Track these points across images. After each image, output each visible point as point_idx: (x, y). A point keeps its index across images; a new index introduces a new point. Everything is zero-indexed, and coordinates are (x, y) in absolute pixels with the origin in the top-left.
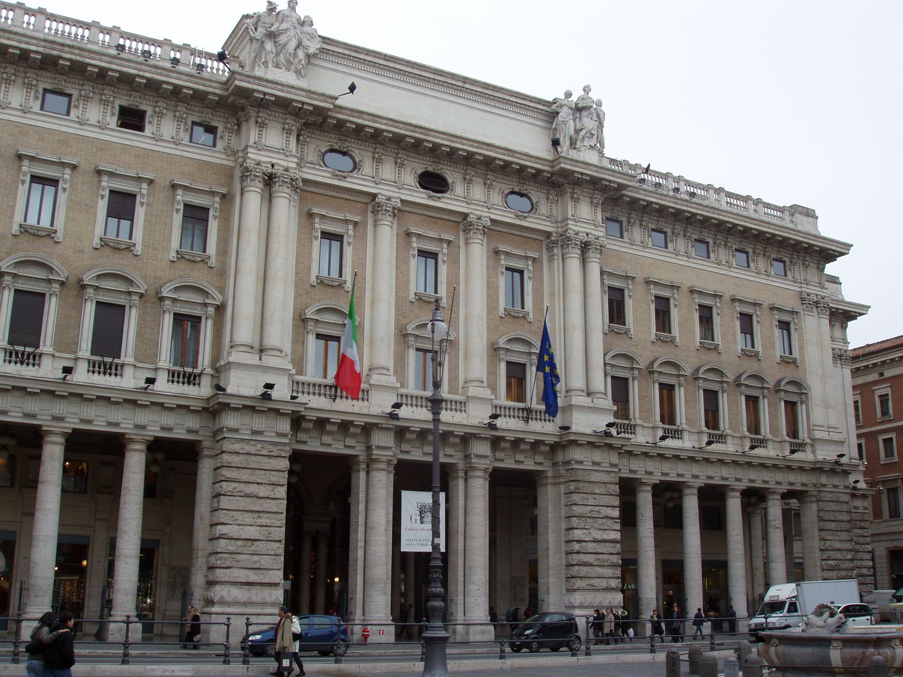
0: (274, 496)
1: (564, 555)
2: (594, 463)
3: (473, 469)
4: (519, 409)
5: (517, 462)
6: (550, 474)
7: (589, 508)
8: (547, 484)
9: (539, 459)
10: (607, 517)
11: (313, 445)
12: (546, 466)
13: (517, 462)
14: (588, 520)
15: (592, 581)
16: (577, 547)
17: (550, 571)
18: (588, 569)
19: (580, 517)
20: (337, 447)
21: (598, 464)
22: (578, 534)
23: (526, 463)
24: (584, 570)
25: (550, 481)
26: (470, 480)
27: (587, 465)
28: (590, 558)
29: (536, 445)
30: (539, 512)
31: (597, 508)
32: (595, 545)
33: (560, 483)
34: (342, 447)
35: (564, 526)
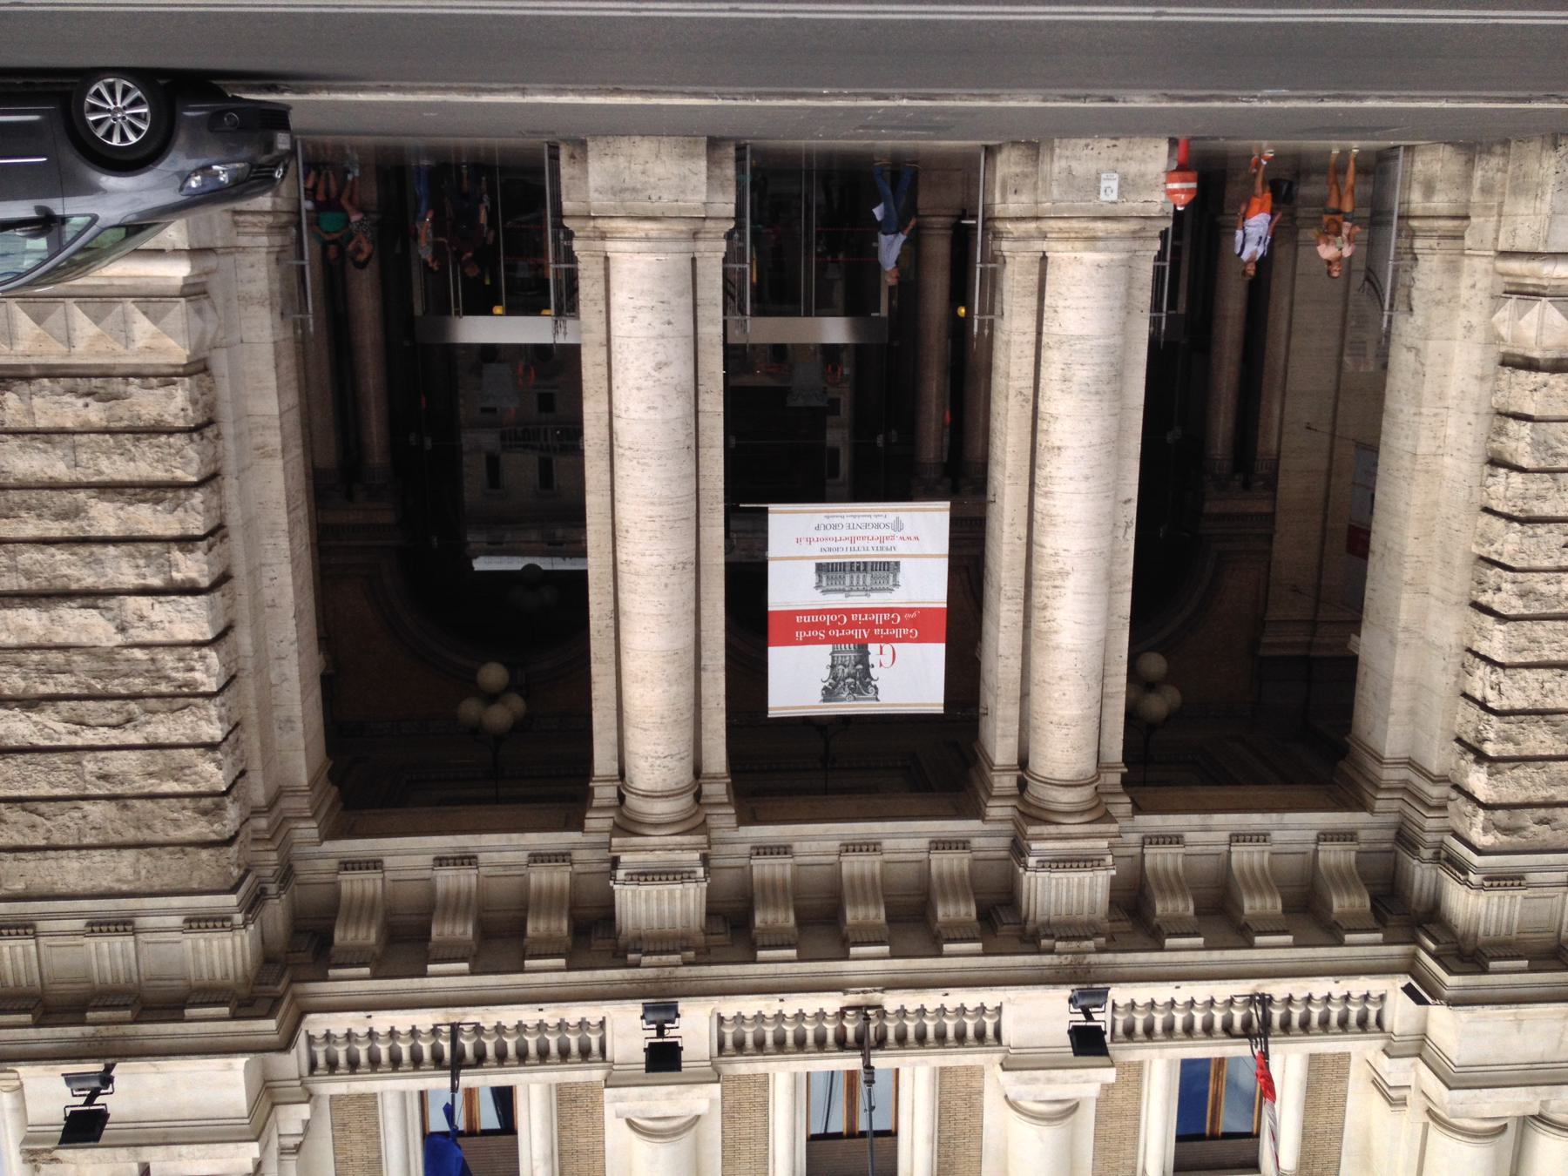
0: (1545, 674)
1: (234, 519)
2: (124, 925)
3: (695, 822)
4: (480, 1058)
5: (467, 859)
6: (307, 830)
7: (133, 737)
8: (312, 784)
9: (357, 884)
10: (29, 703)
11: (1295, 830)
12: (323, 855)
13: (467, 859)
14: (138, 684)
15: (95, 413)
16: (191, 566)
17: (274, 440)
18: (115, 468)
19: (185, 696)
20: (1204, 834)
21: (99, 926)
22: (187, 620)
23: (427, 860)
24: (143, 464)
25: (302, 804)
26: (686, 777)
27: (162, 914)
28: (106, 517)
29: (406, 942)
30: (316, 663)
31: (89, 737)
32: (89, 579)
33: (272, 803)
34: (1188, 837)
35: (244, 639)
